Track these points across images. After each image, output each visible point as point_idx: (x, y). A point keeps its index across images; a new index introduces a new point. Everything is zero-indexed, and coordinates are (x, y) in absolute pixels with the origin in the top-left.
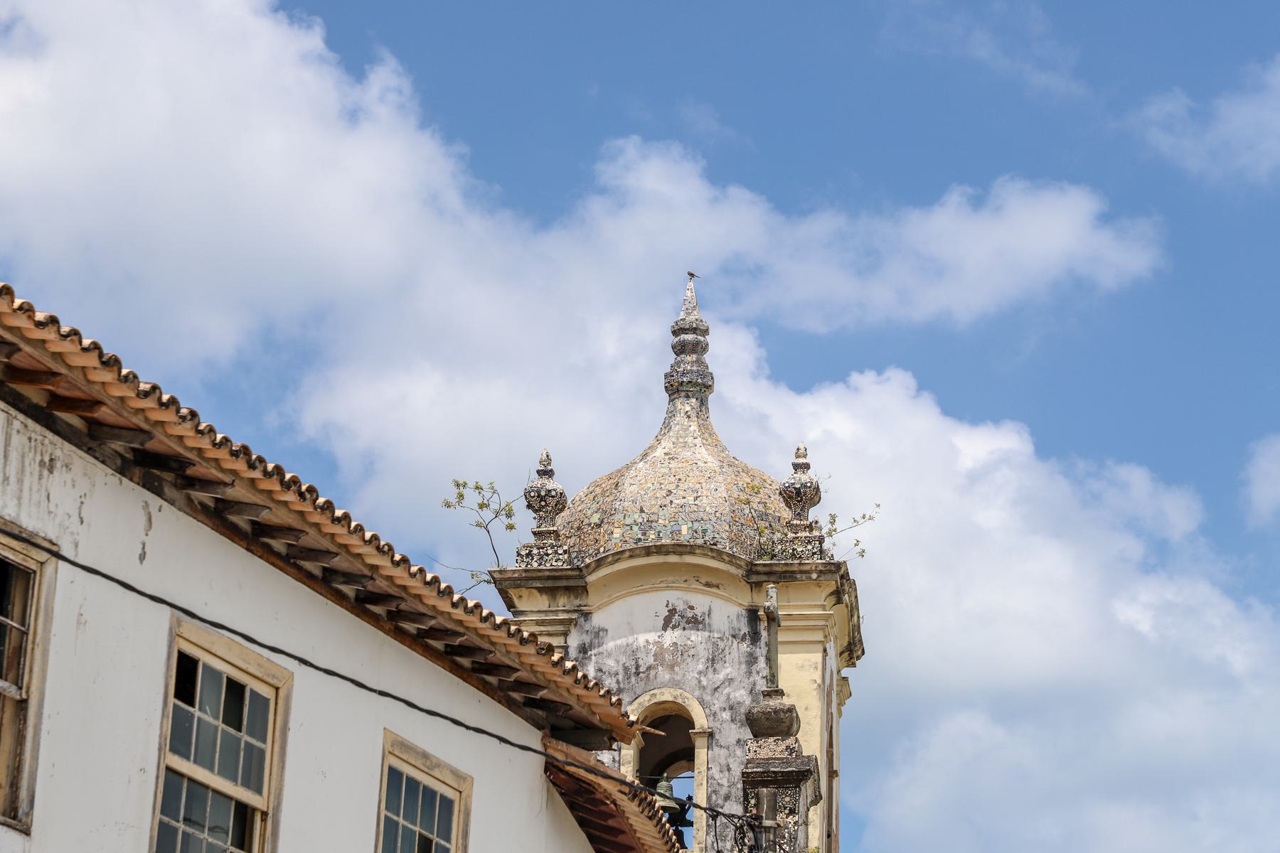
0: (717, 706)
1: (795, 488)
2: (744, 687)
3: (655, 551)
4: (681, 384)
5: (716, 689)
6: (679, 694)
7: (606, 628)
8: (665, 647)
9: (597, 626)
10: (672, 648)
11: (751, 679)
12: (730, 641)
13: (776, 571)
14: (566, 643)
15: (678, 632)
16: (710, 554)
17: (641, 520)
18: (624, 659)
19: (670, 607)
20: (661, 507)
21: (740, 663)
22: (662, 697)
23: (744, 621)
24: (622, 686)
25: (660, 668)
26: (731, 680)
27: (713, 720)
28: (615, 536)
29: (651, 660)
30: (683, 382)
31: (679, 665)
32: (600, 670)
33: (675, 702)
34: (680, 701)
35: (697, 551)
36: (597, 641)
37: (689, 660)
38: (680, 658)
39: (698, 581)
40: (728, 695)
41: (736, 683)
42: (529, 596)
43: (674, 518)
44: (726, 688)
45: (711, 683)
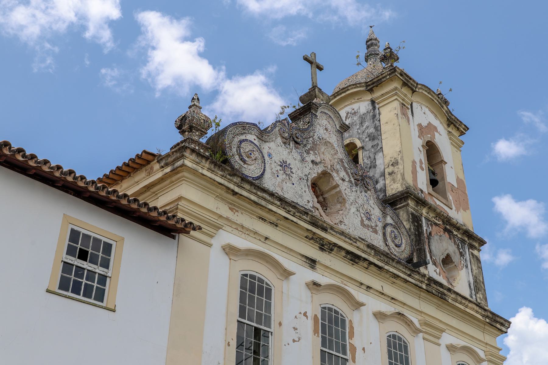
1: (383, 55)
5: (363, 132)
23: (370, 105)
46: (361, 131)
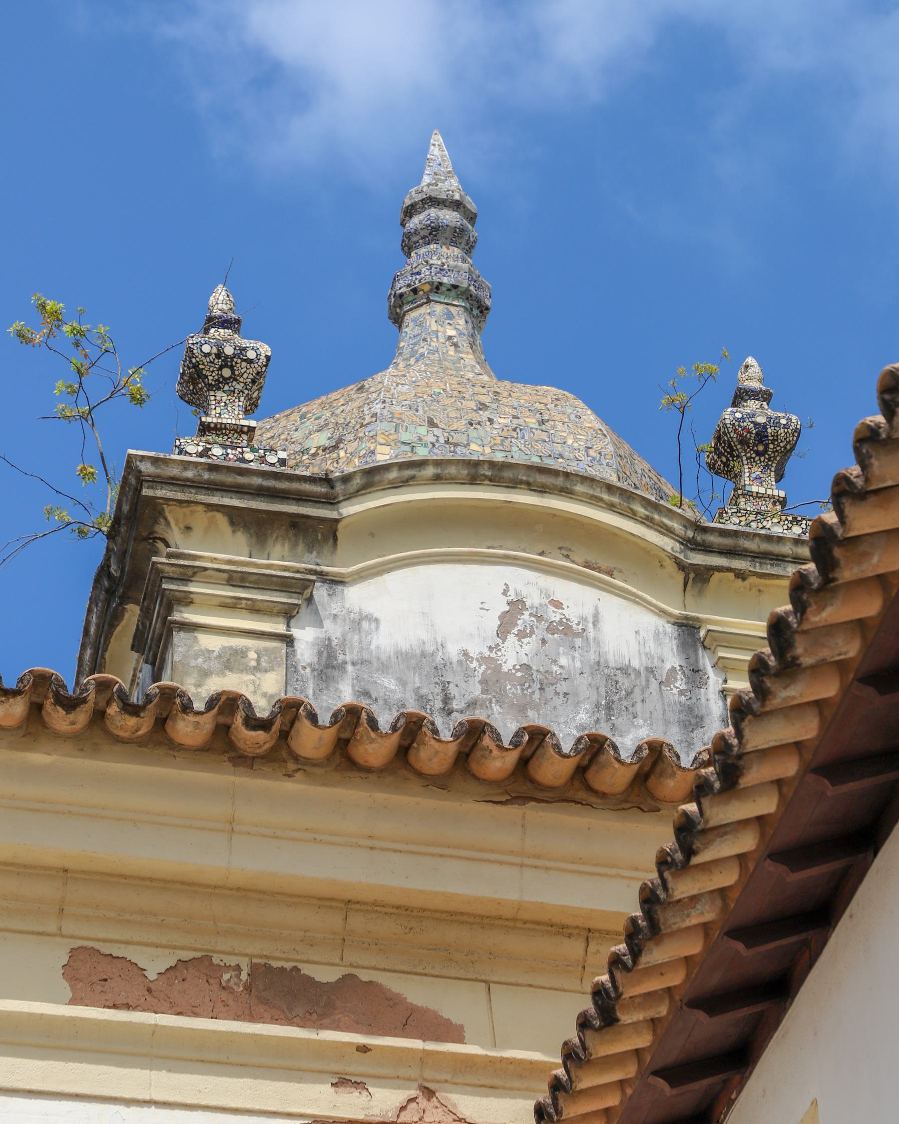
7: (375, 616)
8: (505, 669)
9: (357, 610)
10: (519, 674)
12: (643, 679)
15: (531, 645)
17: (433, 440)
18: (417, 680)
19: (512, 597)
20: (471, 424)
25: (496, 708)
29: (476, 690)
36: (356, 637)
37: (559, 701)
39: (567, 556)
43: (503, 445)
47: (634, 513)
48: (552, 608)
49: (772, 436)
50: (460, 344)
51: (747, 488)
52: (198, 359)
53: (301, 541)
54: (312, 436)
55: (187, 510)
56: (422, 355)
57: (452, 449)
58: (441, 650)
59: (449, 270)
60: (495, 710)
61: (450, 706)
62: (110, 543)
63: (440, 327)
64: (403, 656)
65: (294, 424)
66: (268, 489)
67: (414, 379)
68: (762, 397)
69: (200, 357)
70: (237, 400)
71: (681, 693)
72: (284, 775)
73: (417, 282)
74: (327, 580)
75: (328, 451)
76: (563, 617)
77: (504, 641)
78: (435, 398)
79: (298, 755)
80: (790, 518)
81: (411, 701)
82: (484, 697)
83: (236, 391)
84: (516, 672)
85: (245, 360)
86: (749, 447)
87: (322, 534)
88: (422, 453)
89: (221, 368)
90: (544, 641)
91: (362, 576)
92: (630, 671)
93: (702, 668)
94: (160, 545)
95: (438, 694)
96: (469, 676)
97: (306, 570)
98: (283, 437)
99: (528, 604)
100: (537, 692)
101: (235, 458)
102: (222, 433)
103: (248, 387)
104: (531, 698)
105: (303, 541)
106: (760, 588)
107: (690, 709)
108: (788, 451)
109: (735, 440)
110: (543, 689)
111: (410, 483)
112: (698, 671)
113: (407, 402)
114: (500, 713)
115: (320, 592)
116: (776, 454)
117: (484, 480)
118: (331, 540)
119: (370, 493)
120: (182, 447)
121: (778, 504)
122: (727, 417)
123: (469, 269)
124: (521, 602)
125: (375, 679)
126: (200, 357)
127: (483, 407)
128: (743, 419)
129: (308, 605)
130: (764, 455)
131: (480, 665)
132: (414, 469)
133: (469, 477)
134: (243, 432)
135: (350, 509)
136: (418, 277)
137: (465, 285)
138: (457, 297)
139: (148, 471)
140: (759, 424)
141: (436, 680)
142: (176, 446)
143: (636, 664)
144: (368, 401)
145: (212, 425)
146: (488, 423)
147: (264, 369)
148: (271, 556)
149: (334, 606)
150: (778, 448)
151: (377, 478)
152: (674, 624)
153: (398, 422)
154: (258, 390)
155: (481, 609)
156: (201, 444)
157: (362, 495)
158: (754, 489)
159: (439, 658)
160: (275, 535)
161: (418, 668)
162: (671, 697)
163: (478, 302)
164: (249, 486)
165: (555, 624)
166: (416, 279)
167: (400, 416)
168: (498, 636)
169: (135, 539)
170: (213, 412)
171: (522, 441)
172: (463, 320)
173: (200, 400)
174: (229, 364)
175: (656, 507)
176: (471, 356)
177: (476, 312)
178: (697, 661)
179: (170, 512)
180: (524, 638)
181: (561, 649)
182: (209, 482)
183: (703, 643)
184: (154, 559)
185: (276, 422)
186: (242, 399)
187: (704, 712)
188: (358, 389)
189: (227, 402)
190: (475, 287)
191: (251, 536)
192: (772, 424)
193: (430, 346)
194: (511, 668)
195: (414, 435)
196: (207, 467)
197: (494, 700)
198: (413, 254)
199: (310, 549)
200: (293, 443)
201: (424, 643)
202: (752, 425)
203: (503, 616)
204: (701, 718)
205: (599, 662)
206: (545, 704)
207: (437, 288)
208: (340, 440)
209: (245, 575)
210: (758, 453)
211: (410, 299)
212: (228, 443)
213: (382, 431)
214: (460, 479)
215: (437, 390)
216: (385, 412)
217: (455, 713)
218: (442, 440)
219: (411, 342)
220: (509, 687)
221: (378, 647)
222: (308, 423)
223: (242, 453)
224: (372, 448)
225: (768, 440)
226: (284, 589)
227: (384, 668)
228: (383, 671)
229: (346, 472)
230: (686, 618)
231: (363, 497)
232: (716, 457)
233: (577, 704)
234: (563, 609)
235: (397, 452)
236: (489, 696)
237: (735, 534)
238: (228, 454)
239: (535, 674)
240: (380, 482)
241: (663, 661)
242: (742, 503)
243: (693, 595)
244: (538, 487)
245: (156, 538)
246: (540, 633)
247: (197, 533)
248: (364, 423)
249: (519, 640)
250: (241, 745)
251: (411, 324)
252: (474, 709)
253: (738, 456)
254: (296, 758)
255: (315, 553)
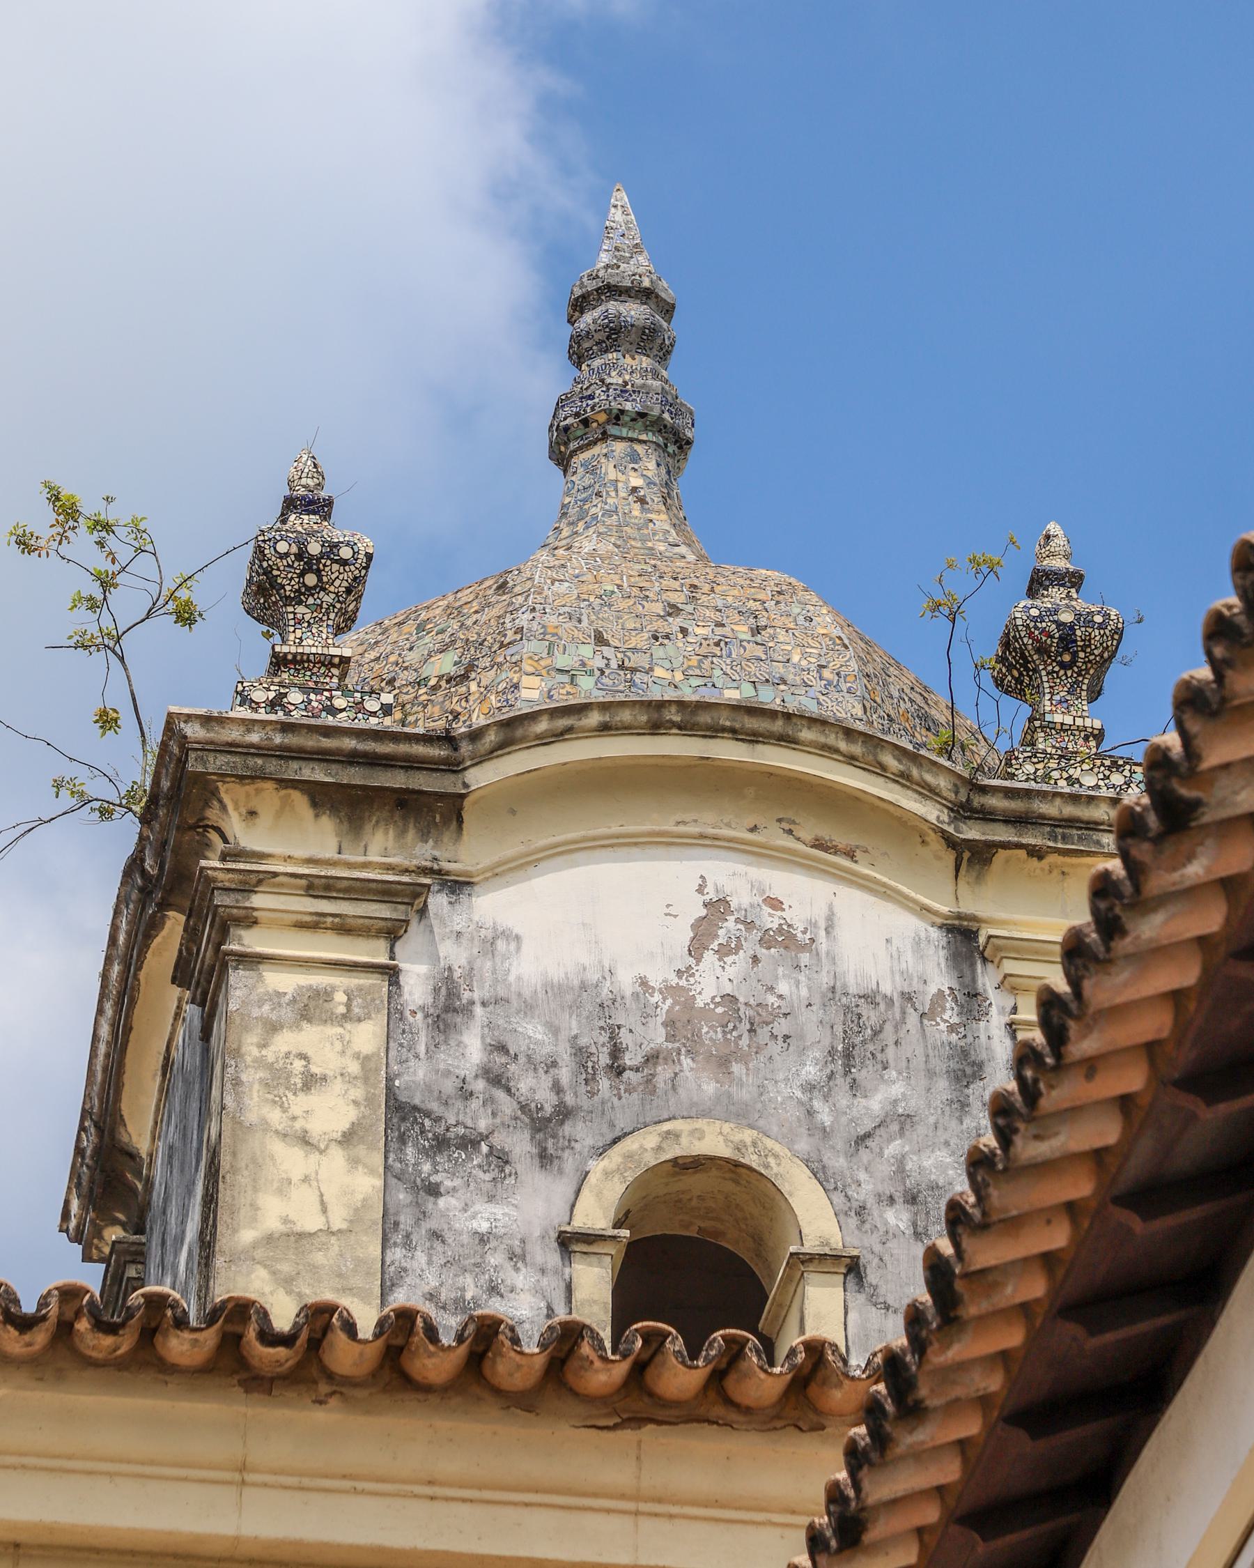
0: (865, 1191)
2: (947, 1143)
3: (677, 718)
4: (617, 418)
5: (862, 1139)
6: (748, 1141)
7: (516, 930)
8: (700, 1003)
9: (489, 924)
10: (720, 1010)
11: (968, 1122)
12: (897, 1009)
13: (1043, 817)
14: (392, 958)
15: (738, 964)
16: (843, 745)
17: (602, 664)
18: (574, 1024)
19: (711, 895)
20: (656, 638)
21: (931, 1074)
22: (696, 1143)
24: (569, 1099)
25: (686, 1062)
26: (906, 1121)
27: (859, 1228)
28: (525, 694)
29: (657, 1036)
30: (622, 412)
31: (744, 1059)
32: (502, 1048)
33: (737, 1165)
34: (752, 1160)
35: (806, 734)
36: (489, 964)
37: (775, 1048)
38: (744, 1042)
39: (790, 832)
40: (901, 1161)
41: (921, 1130)
42: (279, 814)
43: (700, 667)
44: (891, 1139)
45: (844, 1120)
46: (836, 1120)
47: (883, 767)
48: (768, 910)
49: (1082, 640)
50: (648, 499)
51: (1048, 718)
52: (270, 563)
53: (411, 825)
54: (432, 659)
55: (250, 788)
56: (595, 517)
57: (629, 676)
58: (608, 978)
59: (634, 391)
60: (685, 1065)
61: (621, 1062)
62: (144, 829)
63: (620, 474)
64: (555, 990)
65: (407, 639)
66: (365, 755)
67: (577, 571)
68: (1070, 581)
69: (273, 559)
70: (325, 618)
71: (952, 1028)
72: (314, 1402)
73: (588, 409)
74: (447, 881)
75: (453, 683)
76: (783, 922)
77: (698, 961)
78: (606, 600)
79: (332, 1373)
80: (1107, 763)
81: (565, 1056)
82: (670, 1045)
83: (325, 605)
84: (716, 1007)
85: (336, 562)
86: (1049, 657)
87: (442, 816)
88: (587, 688)
89: (302, 575)
90: (755, 959)
91: (501, 872)
92: (878, 999)
93: (981, 991)
94: (214, 836)
95: (603, 1045)
96: (648, 1016)
97: (419, 868)
98: (392, 659)
99: (733, 905)
100: (746, 1036)
101: (321, 707)
102: (304, 668)
103: (341, 599)
104: (737, 1044)
105: (415, 826)
106: (1066, 870)
107: (964, 1053)
108: (1106, 661)
109: (1030, 647)
110: (755, 1031)
111: (566, 737)
112: (975, 995)
113: (567, 609)
114: (692, 1069)
115: (438, 902)
116: (1089, 665)
117: (670, 728)
118: (455, 823)
119: (509, 753)
120: (246, 693)
121: (1091, 739)
122: (1018, 615)
123: (663, 388)
124: (723, 901)
125: (515, 1026)
126: (273, 559)
127: (673, 610)
128: (1041, 618)
129: (420, 920)
130: (1071, 668)
131: (664, 999)
132: (572, 717)
133: (649, 725)
134: (334, 666)
135: (481, 777)
136: (590, 402)
137: (656, 412)
138: (646, 429)
139: (196, 735)
140: (1064, 624)
141: (602, 1023)
142: (237, 693)
143: (886, 988)
144: (511, 609)
145: (290, 657)
146: (680, 636)
147: (363, 572)
148: (369, 848)
149: (457, 919)
150: (1092, 657)
151: (519, 732)
152: (940, 927)
153: (551, 639)
154: (355, 600)
155: (666, 915)
156: (272, 688)
157: (497, 757)
158: (1058, 718)
159: (605, 991)
160: (374, 819)
161: (575, 1007)
162: (937, 1036)
163: (674, 434)
164: (338, 752)
165: (772, 933)
166: (587, 405)
167: (555, 631)
168: (690, 954)
169: (178, 828)
170: (292, 637)
171: (728, 661)
172: (654, 462)
173: (273, 618)
174: (315, 567)
175: (914, 758)
176: (664, 517)
177: (671, 448)
178: (974, 980)
179: (227, 791)
180: (727, 955)
181: (780, 970)
182: (281, 748)
183: (982, 953)
184: (203, 863)
185: (383, 634)
186: (332, 616)
187: (983, 1056)
188: (499, 588)
189: (312, 621)
190: (671, 413)
191: (341, 821)
192: (1082, 624)
193: (606, 504)
194: (709, 1001)
195: (575, 659)
196: (279, 726)
197: (683, 1050)
198: (584, 367)
199: (424, 837)
200: (406, 668)
201: (585, 969)
202: (1054, 626)
203: (697, 925)
204: (980, 1066)
205: (834, 988)
206: (757, 1053)
207: (617, 417)
208: (471, 667)
209: (331, 881)
210: (1063, 665)
211: (579, 433)
212: (311, 684)
213: (531, 654)
214: (636, 728)
215: (609, 588)
216: (535, 625)
217: (628, 1071)
218: (614, 664)
219: (579, 498)
220: (705, 1029)
221: (519, 978)
222: (427, 639)
223: (330, 699)
224: (515, 681)
225: (1077, 646)
226: (386, 899)
227: (528, 1008)
228: (525, 1013)
229: (475, 726)
230: (959, 917)
231: (499, 759)
232: (1004, 670)
233: (803, 1051)
234: (784, 910)
235: (550, 684)
236: (677, 1045)
237: (1028, 794)
238: (310, 701)
239: (742, 1008)
240: (523, 739)
241: (925, 982)
242: (1041, 740)
243: (968, 883)
244: (747, 734)
245: (208, 826)
246: (751, 945)
247: (265, 818)
248: (505, 643)
249: (719, 960)
250: (255, 1362)
251: (581, 470)
252: (655, 1064)
253: (1035, 670)
254: (330, 1376)
255: (431, 842)
